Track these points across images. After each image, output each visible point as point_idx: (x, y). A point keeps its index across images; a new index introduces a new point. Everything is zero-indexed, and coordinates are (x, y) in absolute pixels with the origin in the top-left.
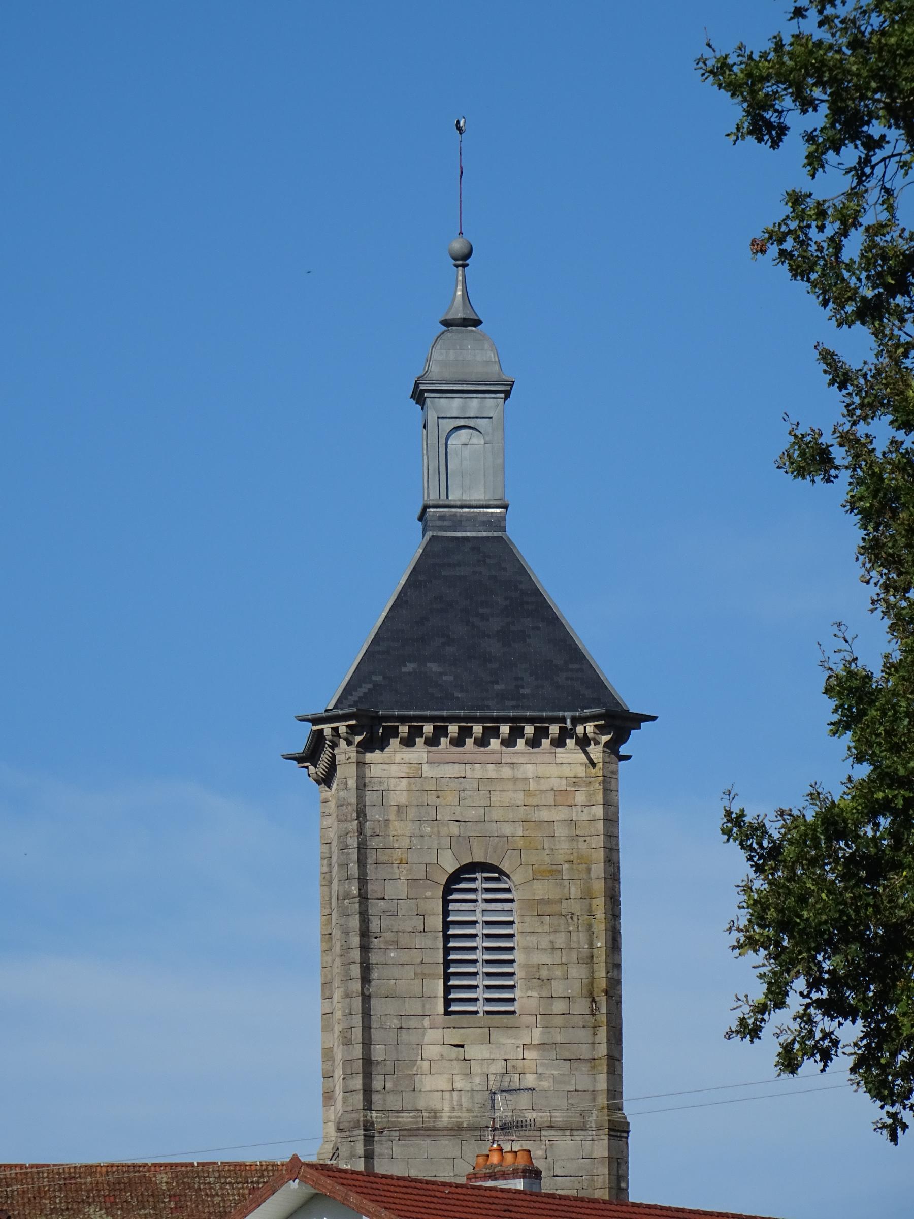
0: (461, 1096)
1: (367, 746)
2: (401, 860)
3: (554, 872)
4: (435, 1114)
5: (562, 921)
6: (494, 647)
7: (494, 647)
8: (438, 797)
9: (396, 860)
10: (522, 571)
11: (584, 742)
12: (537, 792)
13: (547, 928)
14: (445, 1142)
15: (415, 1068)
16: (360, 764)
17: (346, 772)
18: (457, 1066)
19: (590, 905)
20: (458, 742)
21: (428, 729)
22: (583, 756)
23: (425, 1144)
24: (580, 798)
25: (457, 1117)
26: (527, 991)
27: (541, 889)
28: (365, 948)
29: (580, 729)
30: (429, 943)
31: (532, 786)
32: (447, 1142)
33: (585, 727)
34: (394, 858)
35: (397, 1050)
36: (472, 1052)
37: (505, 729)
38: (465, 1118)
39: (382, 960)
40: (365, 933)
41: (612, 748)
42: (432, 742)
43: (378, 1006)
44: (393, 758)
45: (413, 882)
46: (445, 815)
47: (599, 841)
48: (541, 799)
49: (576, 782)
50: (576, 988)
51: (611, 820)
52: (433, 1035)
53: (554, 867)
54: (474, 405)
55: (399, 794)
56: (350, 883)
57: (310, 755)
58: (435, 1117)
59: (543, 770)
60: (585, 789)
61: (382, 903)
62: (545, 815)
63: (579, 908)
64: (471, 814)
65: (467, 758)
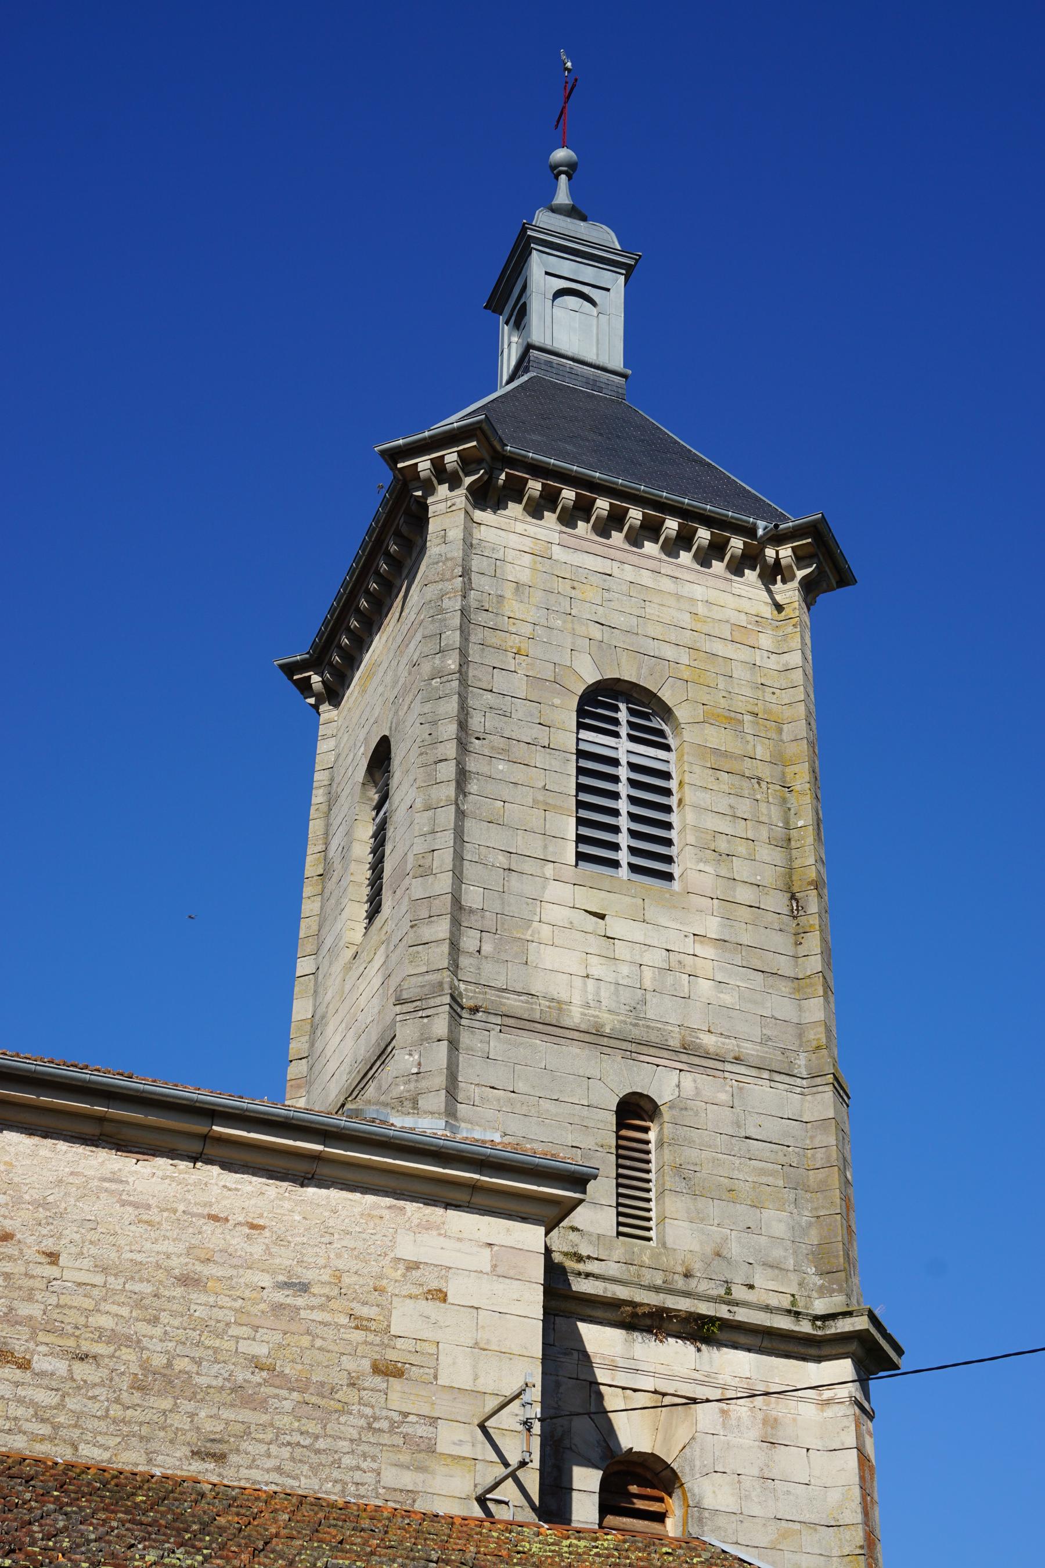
0: (599, 988)
2: (519, 649)
3: (731, 720)
4: (560, 1005)
5: (746, 784)
8: (574, 588)
9: (512, 647)
12: (709, 620)
13: (725, 788)
14: (575, 1049)
15: (530, 932)
18: (595, 945)
19: (783, 774)
22: (766, 593)
25: (593, 1016)
26: (698, 862)
27: (715, 737)
29: (770, 552)
30: (556, 765)
31: (701, 609)
32: (578, 1051)
33: (777, 552)
34: (510, 644)
35: (502, 899)
36: (615, 926)
39: (484, 769)
43: (473, 830)
44: (513, 526)
46: (584, 611)
48: (714, 628)
50: (769, 876)
52: (556, 891)
53: (733, 714)
55: (520, 569)
56: (444, 657)
59: (713, 595)
60: (771, 632)
61: (489, 695)
62: (718, 648)
63: (768, 773)
65: (612, 553)
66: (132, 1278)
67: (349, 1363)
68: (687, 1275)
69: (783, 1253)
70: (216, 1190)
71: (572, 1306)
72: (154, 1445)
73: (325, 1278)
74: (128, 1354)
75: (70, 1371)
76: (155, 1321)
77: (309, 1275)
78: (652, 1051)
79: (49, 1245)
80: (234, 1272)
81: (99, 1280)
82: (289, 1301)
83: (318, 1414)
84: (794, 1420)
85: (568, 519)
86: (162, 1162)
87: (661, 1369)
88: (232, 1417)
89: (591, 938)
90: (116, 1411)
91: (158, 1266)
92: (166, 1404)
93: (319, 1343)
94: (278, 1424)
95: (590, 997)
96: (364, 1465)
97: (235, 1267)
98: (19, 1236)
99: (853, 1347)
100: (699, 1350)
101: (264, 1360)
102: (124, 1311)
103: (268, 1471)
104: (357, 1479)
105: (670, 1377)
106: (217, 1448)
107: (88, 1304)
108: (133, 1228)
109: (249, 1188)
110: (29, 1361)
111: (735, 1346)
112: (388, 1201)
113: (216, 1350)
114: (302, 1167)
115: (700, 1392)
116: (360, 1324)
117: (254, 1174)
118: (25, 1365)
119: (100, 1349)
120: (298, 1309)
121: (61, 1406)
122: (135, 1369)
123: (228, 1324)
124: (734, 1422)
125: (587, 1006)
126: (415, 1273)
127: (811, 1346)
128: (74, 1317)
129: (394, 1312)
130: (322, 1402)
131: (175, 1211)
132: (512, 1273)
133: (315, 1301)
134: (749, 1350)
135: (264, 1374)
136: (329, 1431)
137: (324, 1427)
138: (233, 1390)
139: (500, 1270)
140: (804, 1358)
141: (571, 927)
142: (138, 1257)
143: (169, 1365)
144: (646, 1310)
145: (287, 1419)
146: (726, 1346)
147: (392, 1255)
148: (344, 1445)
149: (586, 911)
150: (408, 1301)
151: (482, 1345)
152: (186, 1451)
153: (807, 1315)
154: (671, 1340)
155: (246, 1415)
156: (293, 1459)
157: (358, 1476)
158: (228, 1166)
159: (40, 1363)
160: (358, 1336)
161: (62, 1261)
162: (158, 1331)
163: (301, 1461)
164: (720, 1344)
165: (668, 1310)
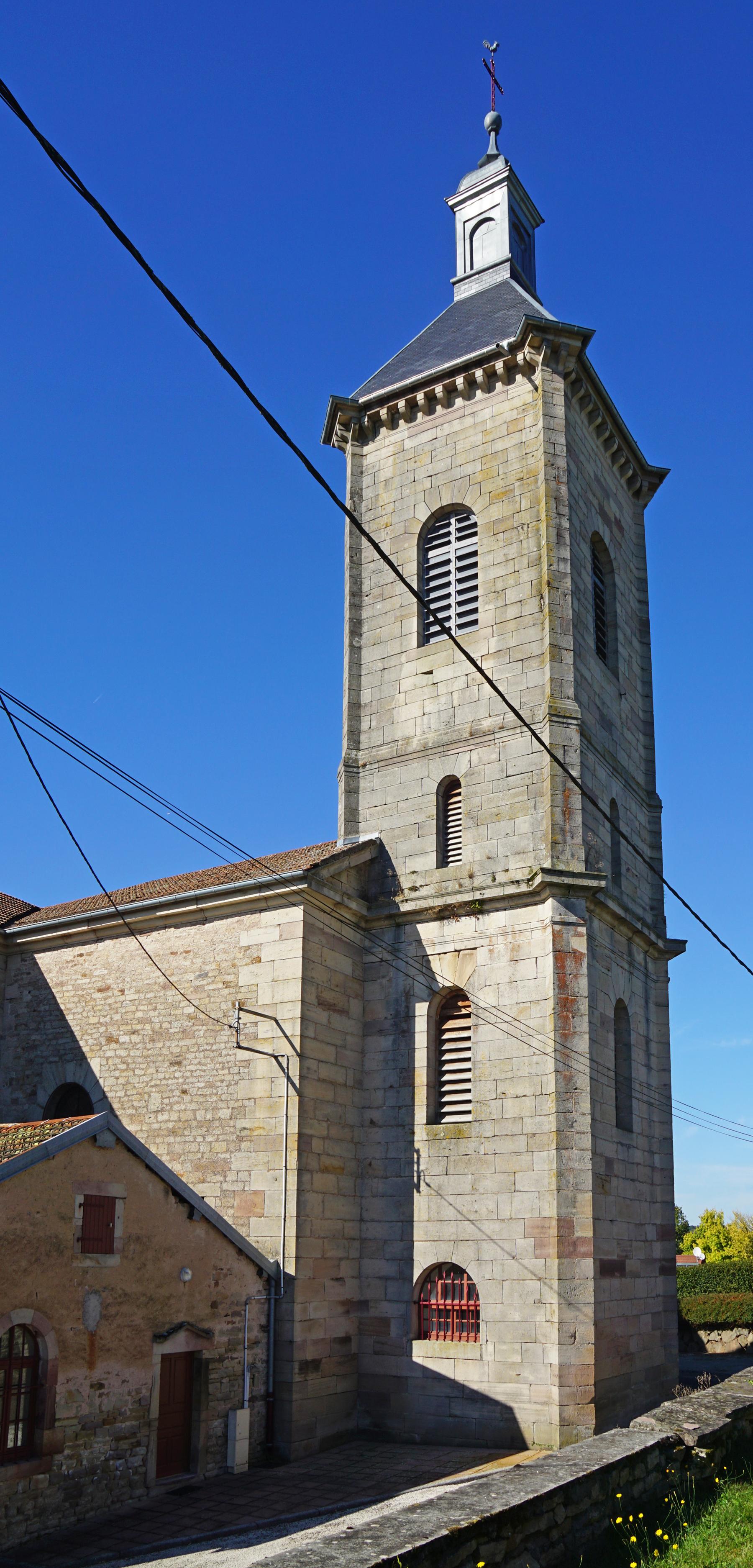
0: (430, 719)
14: (415, 765)
23: (397, 772)
25: (425, 739)
38: (432, 738)
52: (409, 669)
58: (407, 743)
66: (147, 992)
67: (223, 1006)
68: (471, 876)
69: (526, 842)
70: (173, 939)
71: (409, 918)
72: (158, 1064)
73: (214, 967)
74: (147, 1027)
75: (130, 1039)
76: (155, 1009)
77: (208, 968)
78: (454, 746)
79: (121, 986)
80: (180, 977)
81: (136, 997)
82: (201, 983)
83: (213, 1034)
84: (529, 943)
85: (410, 418)
86: (155, 934)
87: (457, 937)
88: (183, 1044)
89: (425, 689)
90: (145, 1053)
91: (156, 983)
92: (160, 1045)
93: (212, 1000)
94: (199, 1043)
95: (425, 727)
96: (230, 1053)
97: (181, 974)
98: (112, 986)
99: (547, 892)
100: (478, 919)
101: (192, 1015)
102: (145, 1008)
103: (196, 1065)
104: (228, 1060)
105: (462, 940)
106: (178, 1059)
107: (134, 1008)
108: (147, 969)
109: (185, 934)
110: (118, 1039)
111: (497, 910)
112: (237, 919)
113: (176, 1015)
114: (199, 916)
115: (477, 943)
116: (227, 985)
117: (186, 927)
118: (117, 1042)
119: (139, 1027)
120: (203, 986)
121: (129, 1055)
122: (150, 1032)
123: (180, 1002)
124: (496, 955)
125: (424, 733)
126: (248, 952)
127: (535, 896)
128: (130, 1016)
129: (240, 975)
130: (214, 1028)
131: (160, 955)
132: (289, 937)
133: (210, 980)
134: (505, 910)
135: (193, 1021)
136: (217, 1041)
137: (215, 1040)
138: (182, 1032)
139: (283, 937)
140: (536, 904)
141: (415, 687)
142: (148, 982)
143: (161, 1027)
144: (437, 910)
145: (202, 1039)
146: (492, 911)
147: (238, 946)
148: (223, 1045)
149: (423, 673)
150: (246, 967)
151: (276, 979)
152: (167, 1064)
153: (523, 880)
154: (463, 918)
155: (188, 1042)
156: (204, 1057)
157: (228, 1059)
158: (177, 926)
159: (123, 1039)
160: (226, 991)
161: (126, 992)
162: (157, 1013)
163: (207, 1057)
164: (488, 912)
165: (450, 905)
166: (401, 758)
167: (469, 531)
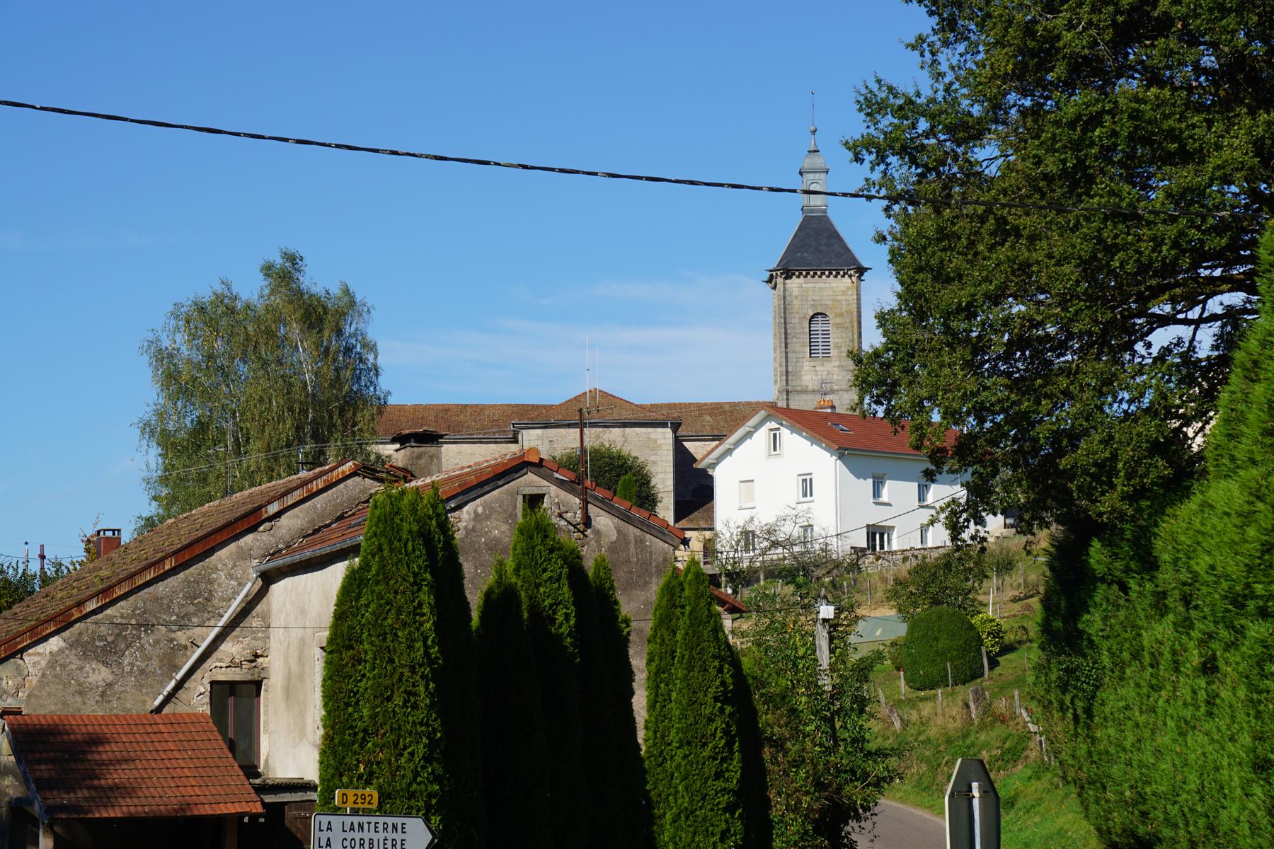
1: (786, 278)
3: (842, 315)
4: (807, 387)
6: (824, 248)
7: (824, 248)
10: (832, 225)
11: (850, 276)
16: (784, 284)
17: (780, 286)
20: (813, 277)
21: (804, 273)
23: (804, 396)
24: (850, 293)
27: (838, 320)
28: (786, 338)
36: (818, 368)
37: (827, 273)
38: (816, 388)
40: (786, 334)
41: (859, 278)
42: (806, 277)
45: (800, 318)
46: (809, 298)
47: (855, 306)
49: (848, 288)
51: (859, 299)
52: (807, 363)
54: (817, 176)
55: (796, 292)
57: (770, 280)
62: (839, 298)
64: (817, 298)
166: (805, 392)
167: (826, 322)
